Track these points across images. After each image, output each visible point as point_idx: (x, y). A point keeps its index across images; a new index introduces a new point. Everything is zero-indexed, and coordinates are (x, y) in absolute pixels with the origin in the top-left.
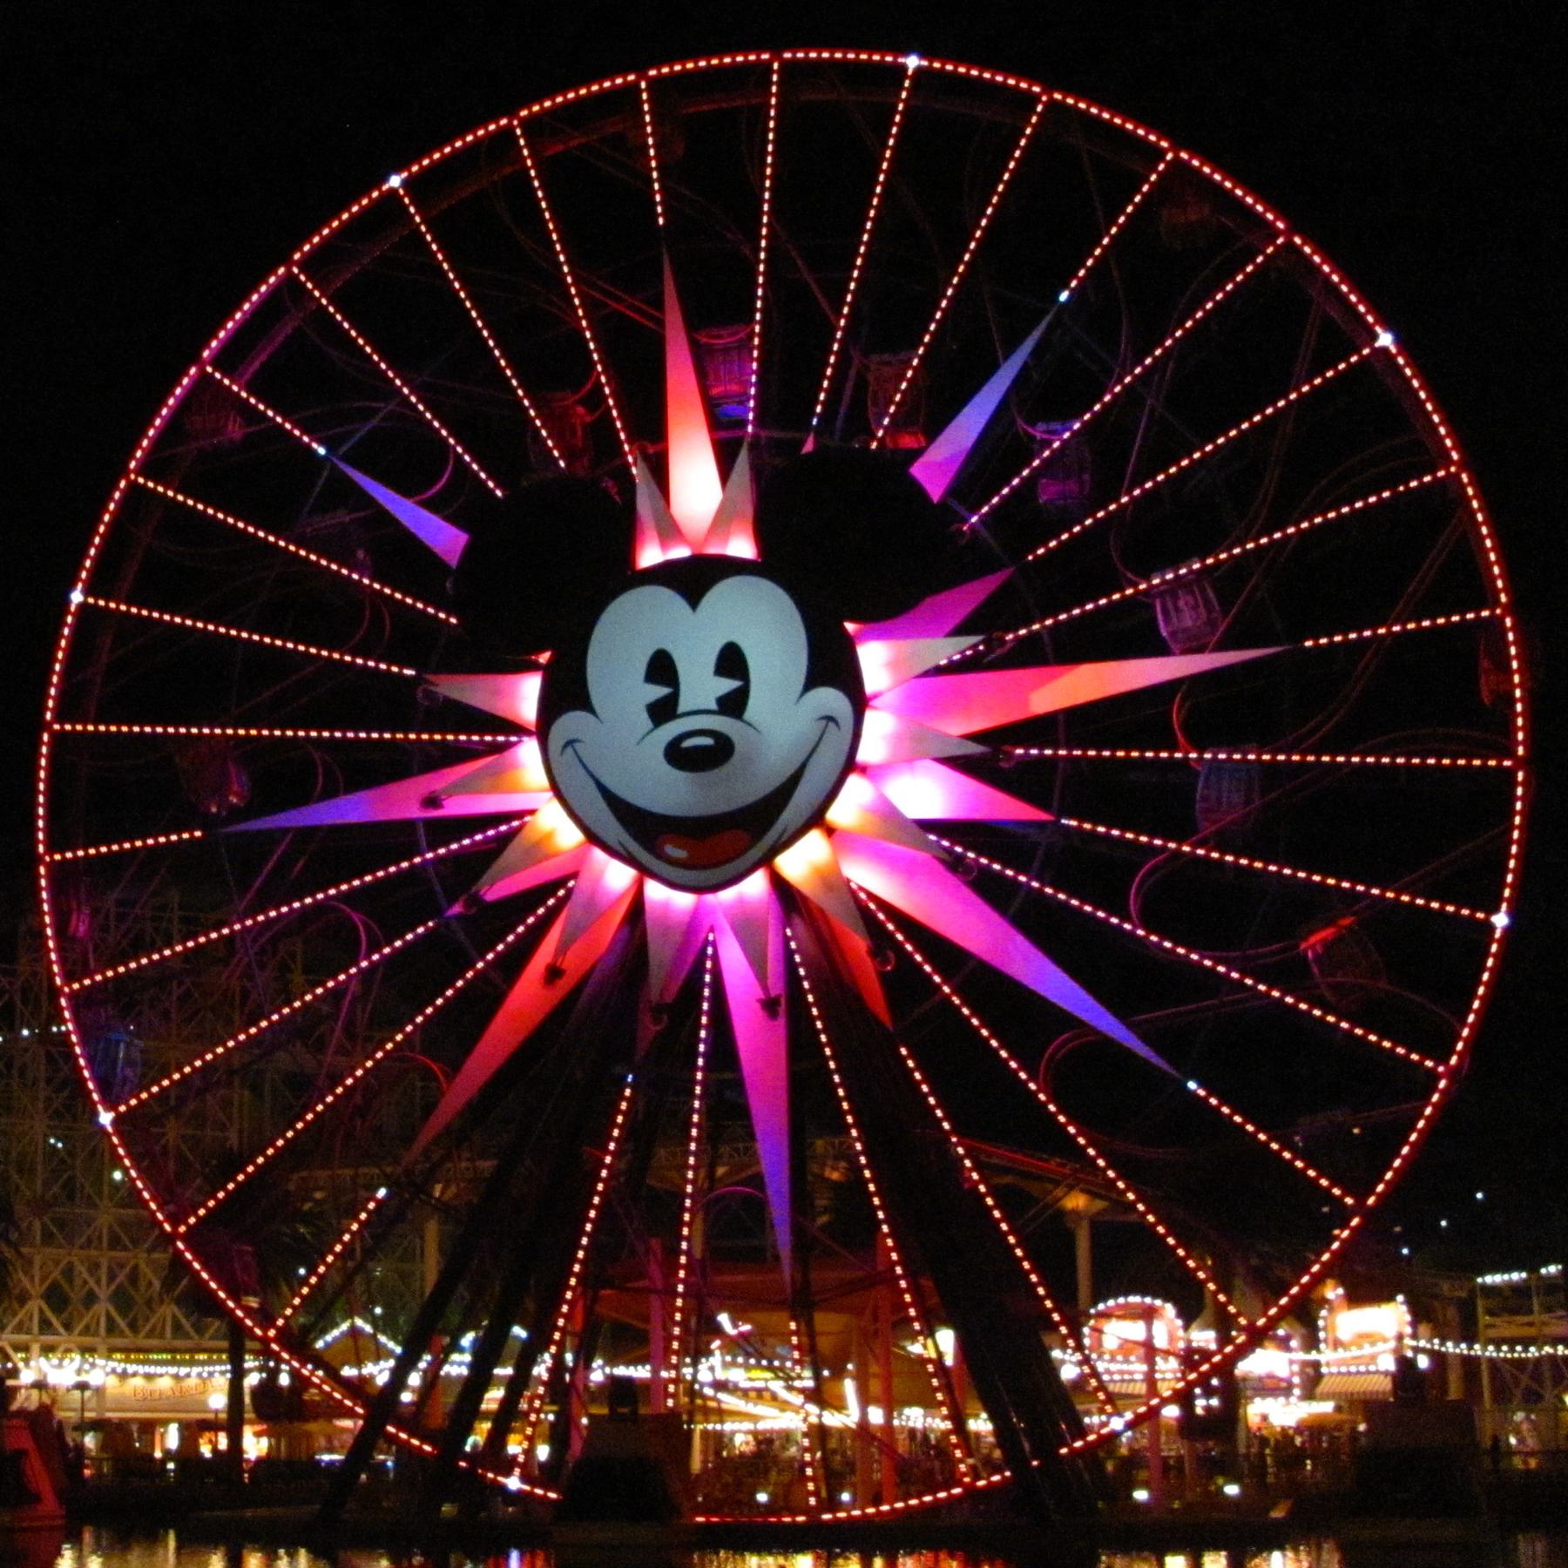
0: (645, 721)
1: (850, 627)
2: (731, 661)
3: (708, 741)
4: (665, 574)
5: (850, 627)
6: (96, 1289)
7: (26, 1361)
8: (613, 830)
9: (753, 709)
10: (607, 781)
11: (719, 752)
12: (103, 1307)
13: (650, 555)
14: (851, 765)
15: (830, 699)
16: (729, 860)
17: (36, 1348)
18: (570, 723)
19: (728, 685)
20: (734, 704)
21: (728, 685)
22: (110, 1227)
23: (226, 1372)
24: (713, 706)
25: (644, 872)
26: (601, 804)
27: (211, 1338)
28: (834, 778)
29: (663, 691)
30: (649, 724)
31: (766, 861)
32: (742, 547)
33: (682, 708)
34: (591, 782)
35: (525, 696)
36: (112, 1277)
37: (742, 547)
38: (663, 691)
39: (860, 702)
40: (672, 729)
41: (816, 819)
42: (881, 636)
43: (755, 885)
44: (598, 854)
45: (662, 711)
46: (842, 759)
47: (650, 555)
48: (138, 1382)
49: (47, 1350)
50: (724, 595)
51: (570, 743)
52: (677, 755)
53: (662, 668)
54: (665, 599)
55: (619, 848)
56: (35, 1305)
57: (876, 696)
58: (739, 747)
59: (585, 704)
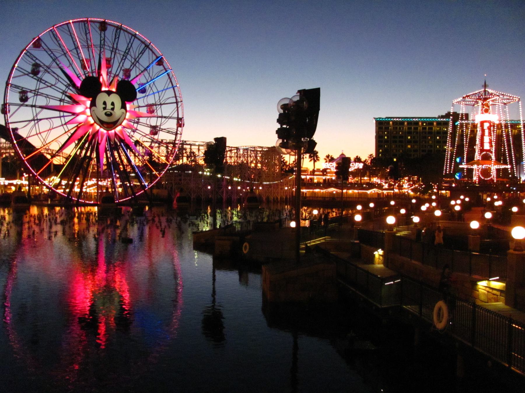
0: (102, 109)
1: (126, 102)
2: (113, 104)
3: (109, 113)
4: (105, 92)
5: (126, 102)
13: (104, 89)
14: (125, 119)
15: (123, 110)
18: (93, 108)
19: (112, 107)
20: (113, 109)
21: (112, 107)
24: (110, 109)
25: (101, 127)
26: (97, 118)
29: (104, 106)
32: (114, 90)
35: (88, 103)
37: (114, 90)
38: (104, 106)
39: (126, 111)
40: (106, 111)
41: (121, 124)
43: (113, 131)
44: (95, 124)
45: (105, 108)
47: (104, 89)
50: (112, 95)
51: (93, 111)
52: (106, 114)
53: (105, 103)
54: (106, 95)
58: (113, 114)
59: (95, 106)
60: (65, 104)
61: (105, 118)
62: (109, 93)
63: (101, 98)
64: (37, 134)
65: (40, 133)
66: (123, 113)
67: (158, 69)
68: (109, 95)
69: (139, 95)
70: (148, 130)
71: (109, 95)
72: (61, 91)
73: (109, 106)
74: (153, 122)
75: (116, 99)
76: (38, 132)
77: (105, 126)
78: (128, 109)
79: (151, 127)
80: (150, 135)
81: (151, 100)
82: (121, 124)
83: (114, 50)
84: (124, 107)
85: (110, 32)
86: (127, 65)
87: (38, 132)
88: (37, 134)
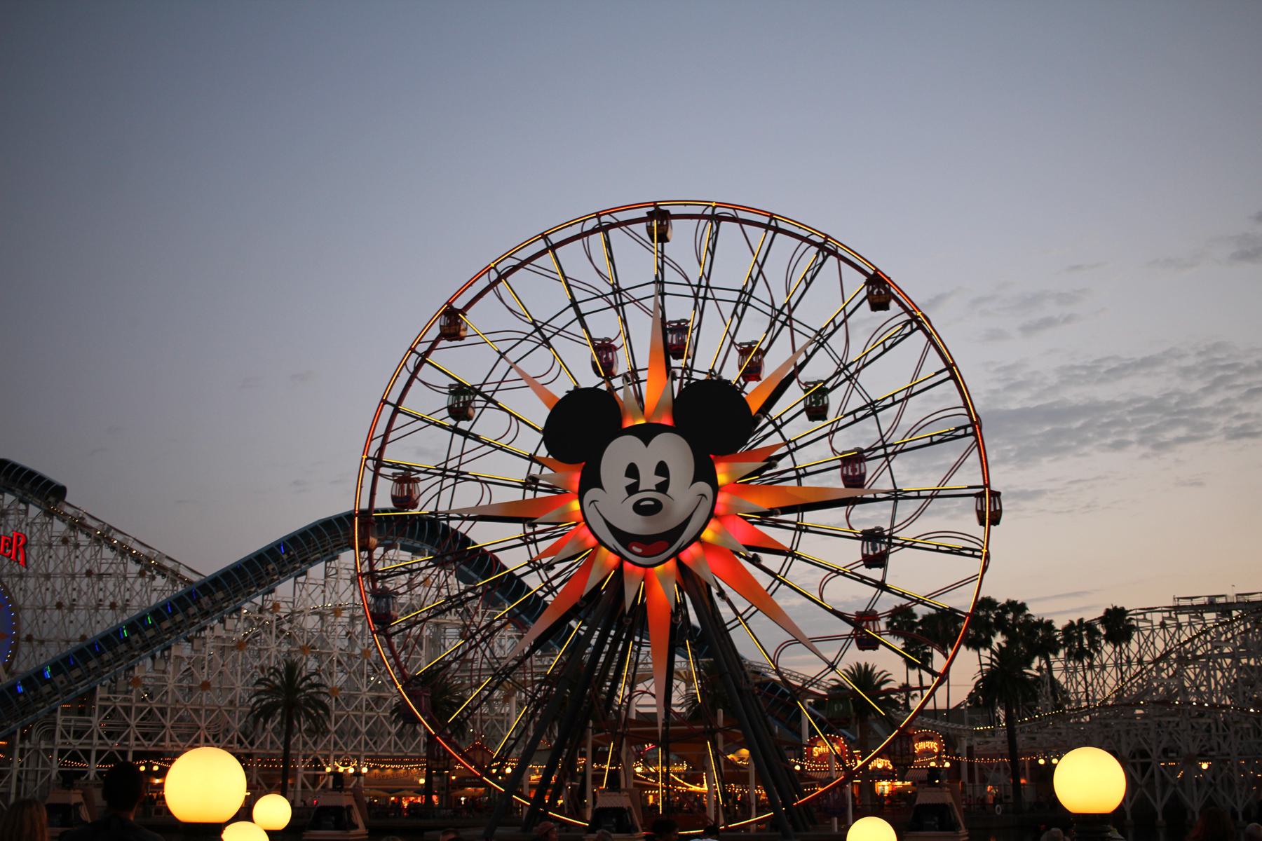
1: (711, 456)
2: (662, 469)
3: (652, 503)
4: (636, 431)
5: (711, 456)
6: (359, 727)
7: (327, 763)
8: (610, 540)
9: (670, 491)
10: (608, 519)
11: (656, 508)
12: (363, 737)
14: (712, 515)
15: (704, 487)
16: (661, 553)
17: (332, 758)
18: (592, 494)
19: (661, 479)
20: (662, 488)
21: (661, 479)
22: (367, 700)
23: (422, 768)
24: (654, 488)
27: (411, 752)
28: (705, 519)
29: (632, 481)
30: (627, 495)
31: (676, 555)
32: (667, 421)
33: (640, 489)
34: (602, 520)
36: (367, 723)
37: (667, 421)
38: (633, 481)
39: (716, 488)
42: (725, 461)
44: (604, 549)
45: (632, 490)
46: (708, 513)
47: (628, 423)
48: (389, 771)
49: (337, 758)
50: (660, 440)
51: (593, 501)
52: (638, 508)
53: (632, 471)
55: (613, 547)
56: (333, 737)
57: (723, 486)
59: (599, 485)
60: (539, 495)
61: (634, 524)
62: (647, 433)
66: (703, 495)
67: (867, 321)
68: (647, 444)
70: (852, 552)
71: (647, 444)
73: (649, 480)
74: (870, 516)
77: (639, 551)
78: (722, 479)
79: (871, 536)
80: (863, 571)
81: (846, 441)
82: (697, 538)
83: (701, 293)
84: (704, 473)
85: (682, 233)
86: (753, 328)
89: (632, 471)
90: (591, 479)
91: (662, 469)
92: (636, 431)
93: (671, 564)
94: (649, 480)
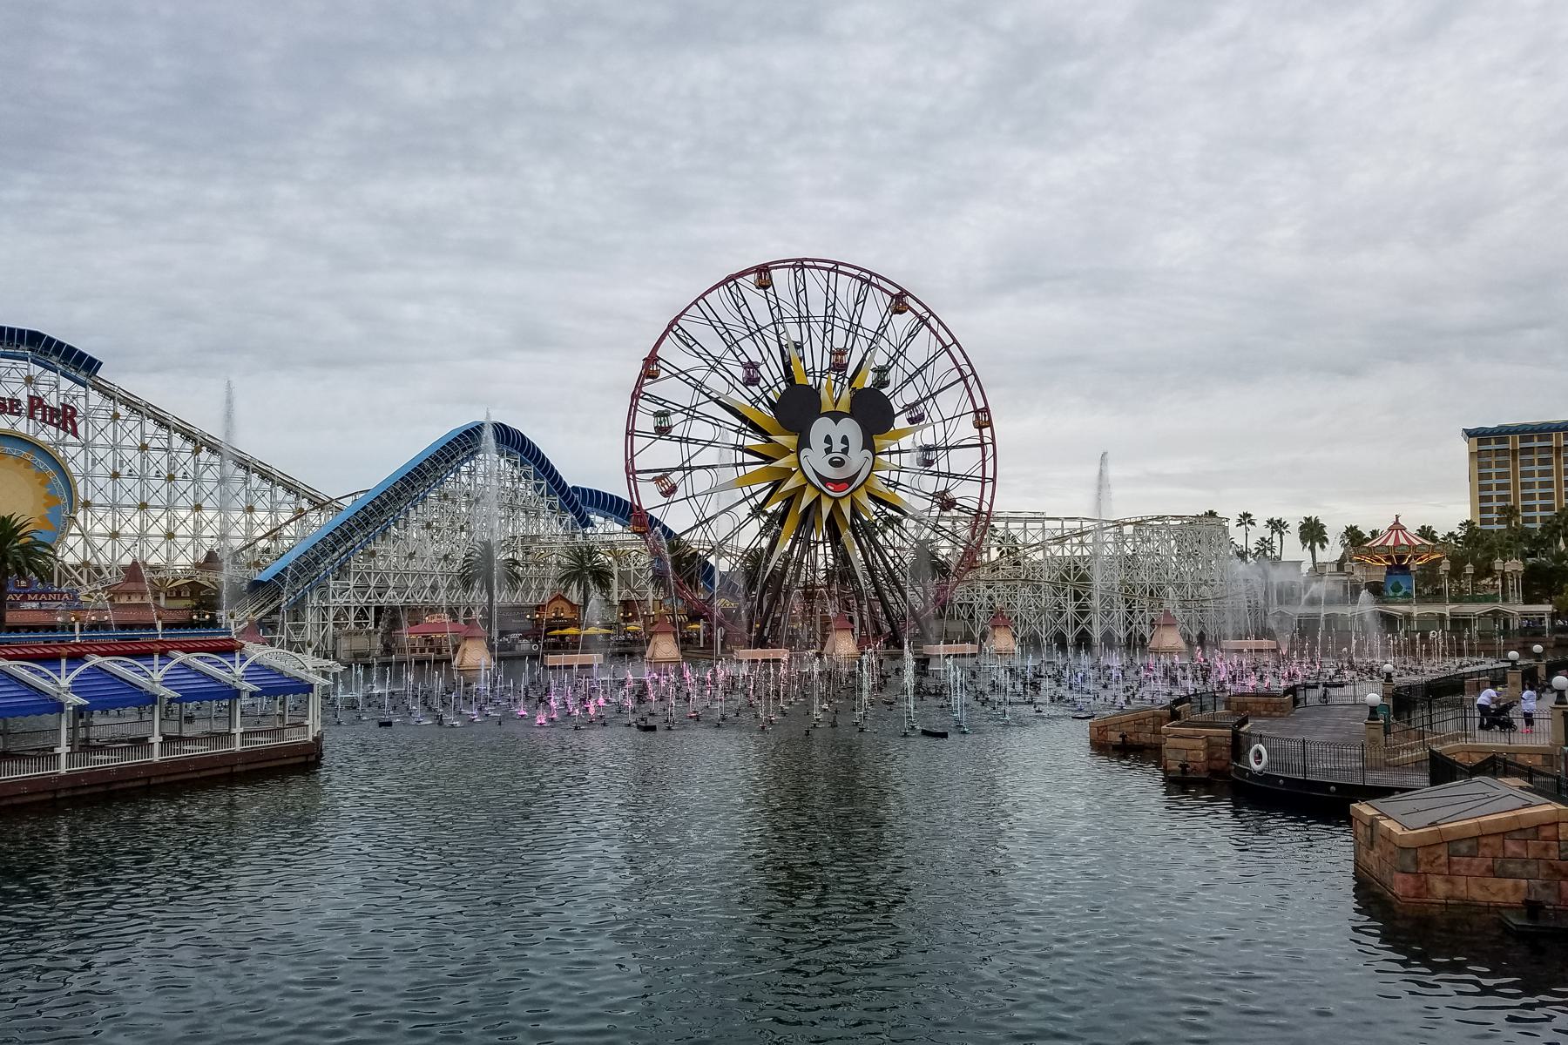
2: (845, 440)
4: (827, 414)
15: (868, 453)
18: (804, 452)
20: (845, 451)
45: (828, 451)
50: (845, 421)
53: (828, 439)
54: (828, 421)
61: (830, 472)
62: (836, 416)
63: (820, 428)
64: (687, 498)
65: (694, 496)
69: (901, 422)
72: (736, 428)
73: (838, 446)
75: (850, 428)
76: (690, 494)
84: (868, 444)
87: (690, 494)
88: (687, 498)
89: (828, 439)
90: (804, 443)
91: (845, 440)
92: (827, 414)
93: (849, 498)
94: (838, 446)
